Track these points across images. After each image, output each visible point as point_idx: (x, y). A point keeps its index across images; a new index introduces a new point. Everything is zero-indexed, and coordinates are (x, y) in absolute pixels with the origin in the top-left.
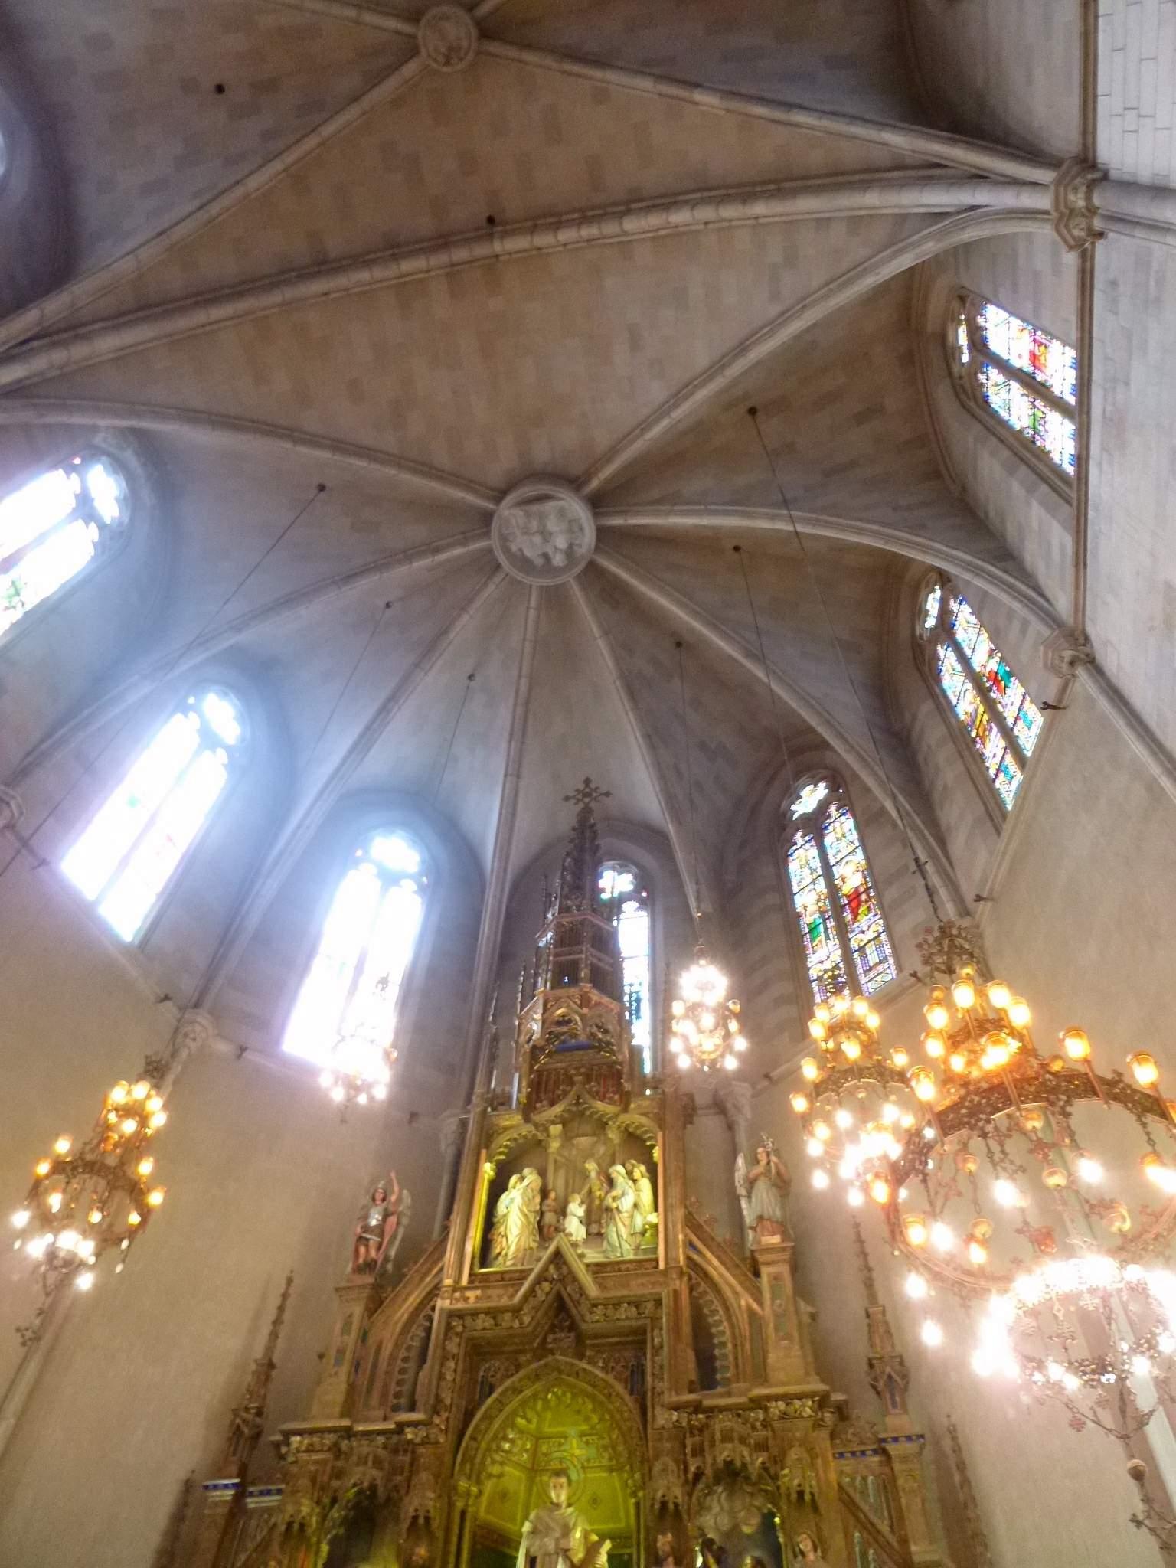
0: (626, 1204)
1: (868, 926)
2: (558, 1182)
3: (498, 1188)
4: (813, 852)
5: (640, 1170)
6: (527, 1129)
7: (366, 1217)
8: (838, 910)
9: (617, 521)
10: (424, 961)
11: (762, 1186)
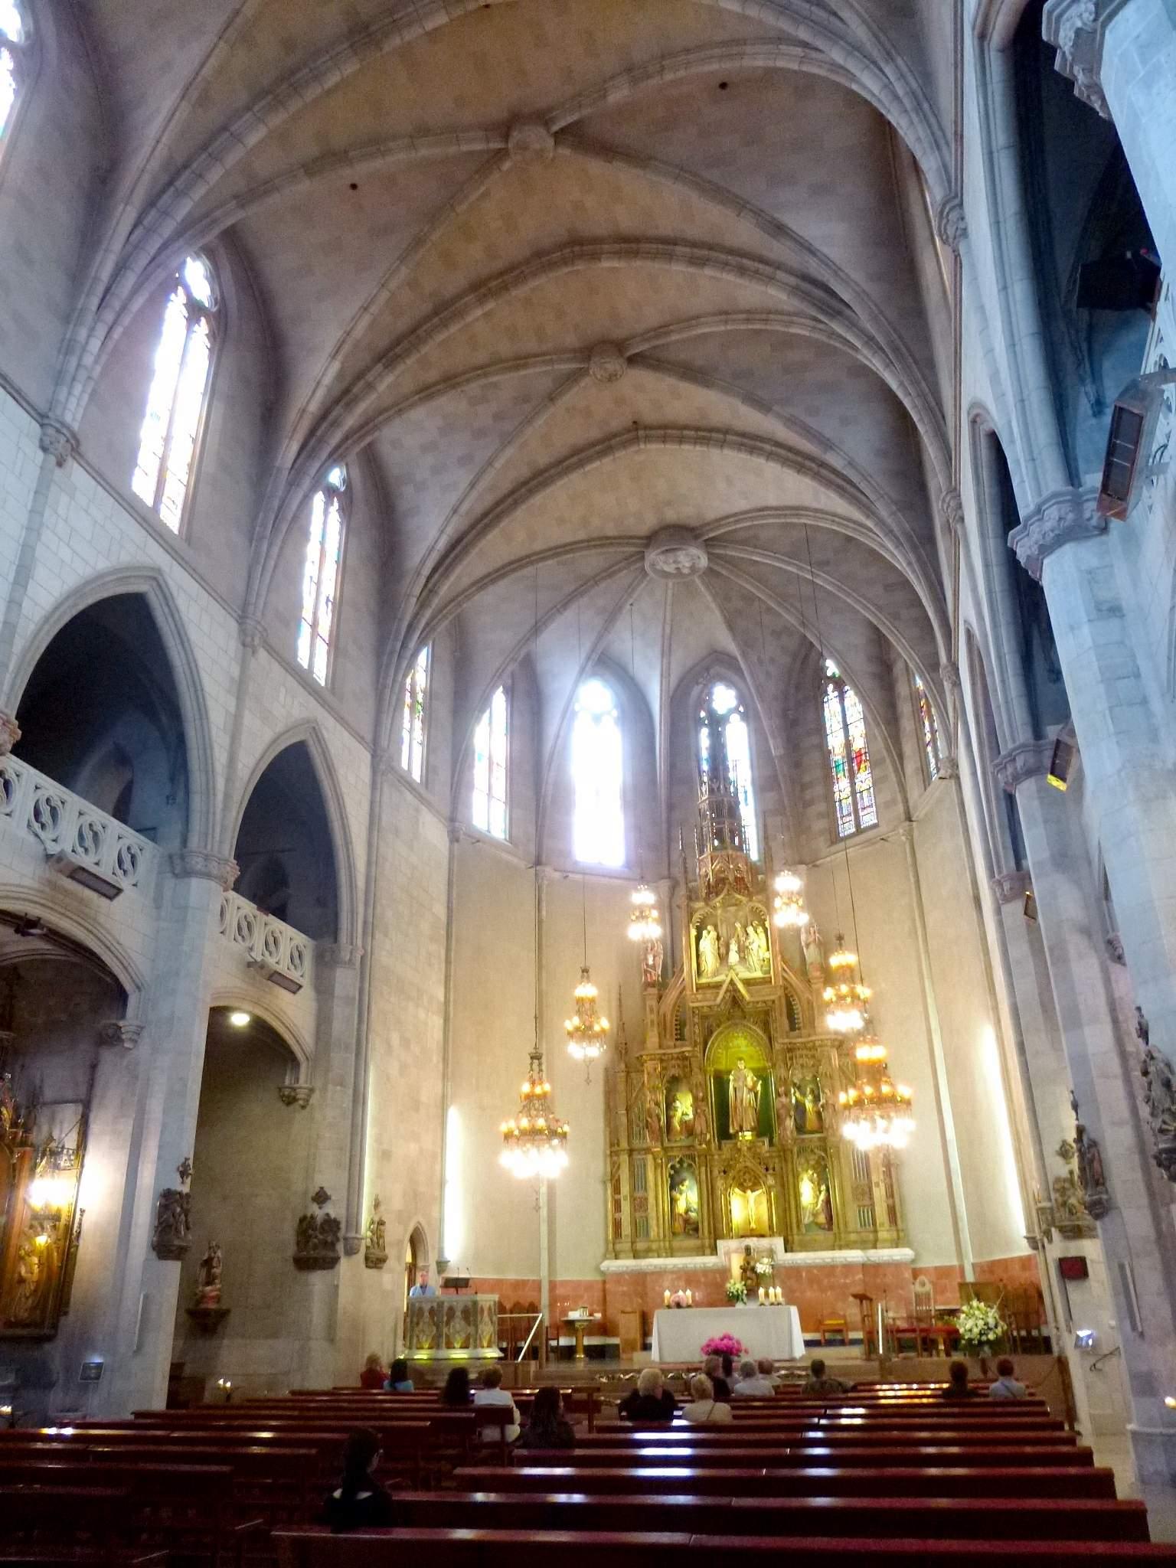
0: (754, 947)
1: (864, 779)
2: (723, 931)
3: (698, 938)
4: (839, 708)
5: (760, 930)
6: (708, 909)
7: (646, 959)
8: (850, 760)
9: (717, 551)
10: (629, 780)
11: (812, 947)
